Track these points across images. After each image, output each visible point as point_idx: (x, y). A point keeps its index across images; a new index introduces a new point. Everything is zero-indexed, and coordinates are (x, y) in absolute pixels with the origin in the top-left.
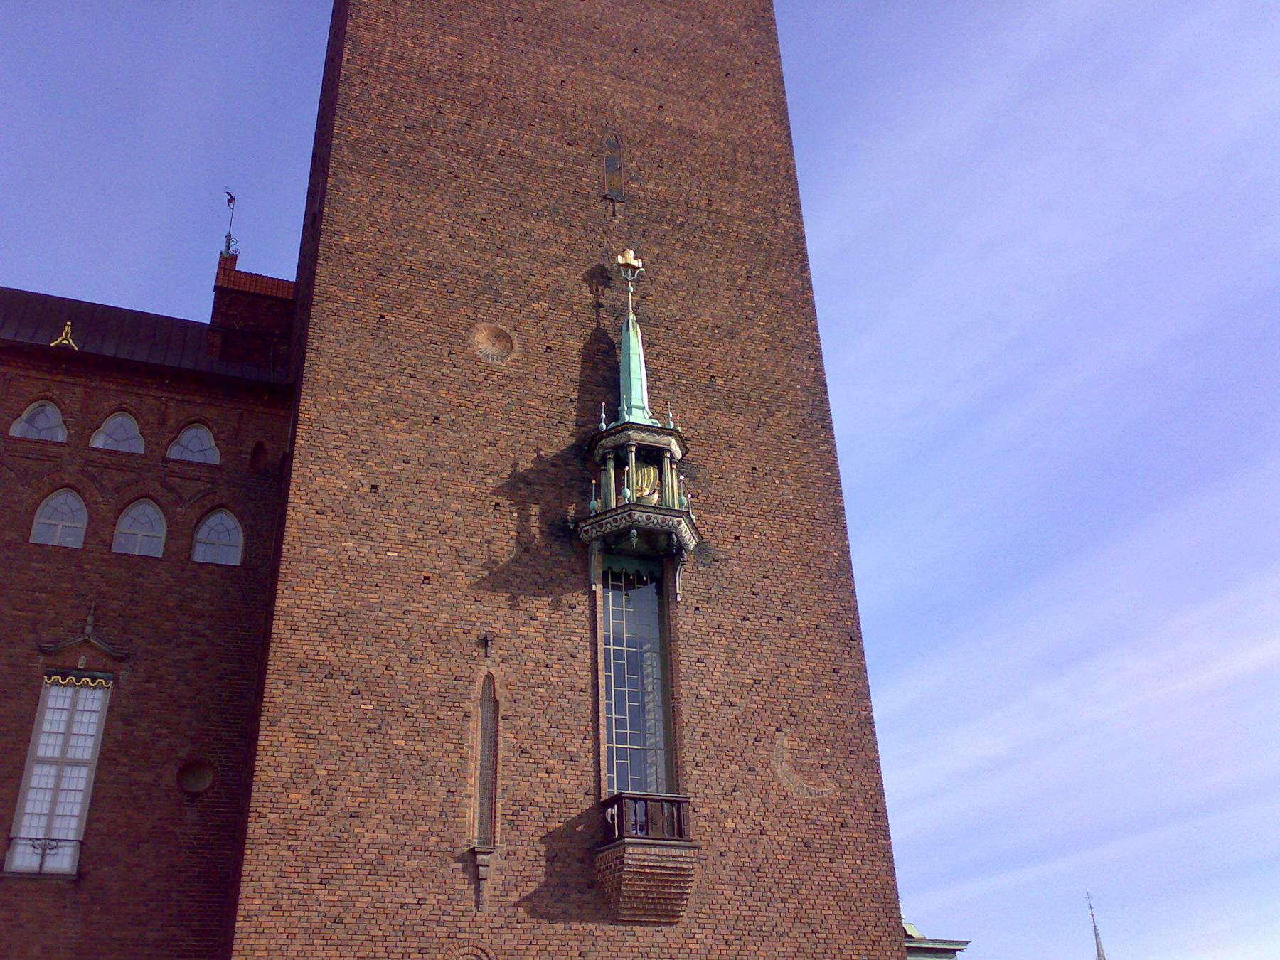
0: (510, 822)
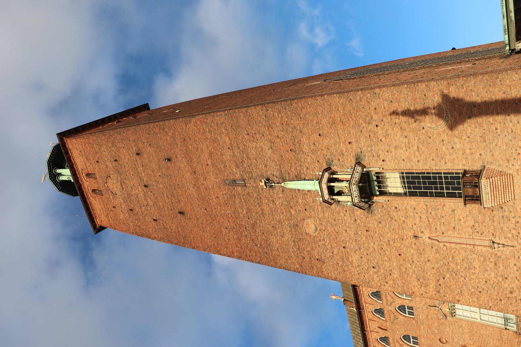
0: (481, 234)
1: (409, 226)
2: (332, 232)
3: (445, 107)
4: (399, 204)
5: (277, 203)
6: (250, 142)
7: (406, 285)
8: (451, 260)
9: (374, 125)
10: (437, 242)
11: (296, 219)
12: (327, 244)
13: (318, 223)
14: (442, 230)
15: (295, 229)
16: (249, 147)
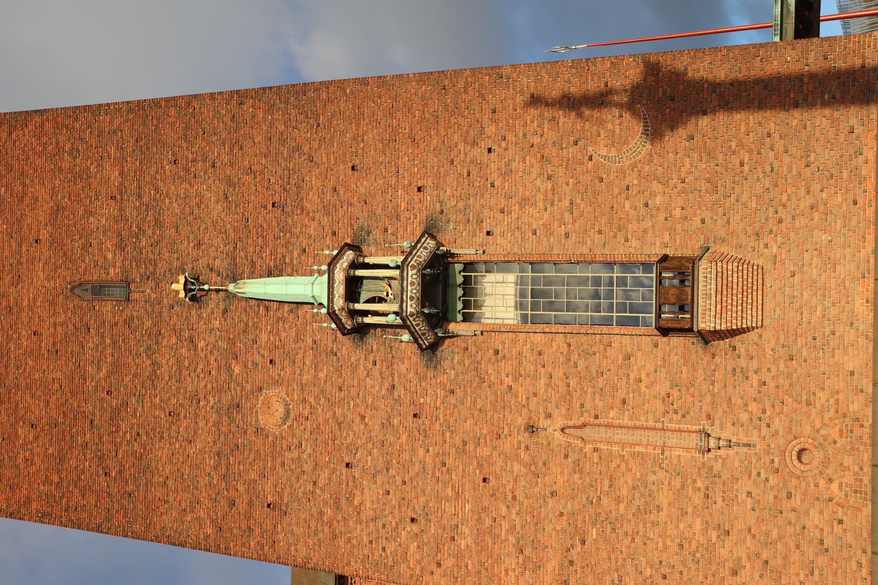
1: (520, 399)
2: (326, 421)
3: (643, 112)
4: (507, 341)
5: (201, 344)
7: (487, 569)
8: (606, 489)
9: (483, 148)
10: (578, 442)
11: (239, 389)
12: (305, 456)
13: (296, 397)
14: (595, 407)
15: (229, 418)
16: (168, 194)
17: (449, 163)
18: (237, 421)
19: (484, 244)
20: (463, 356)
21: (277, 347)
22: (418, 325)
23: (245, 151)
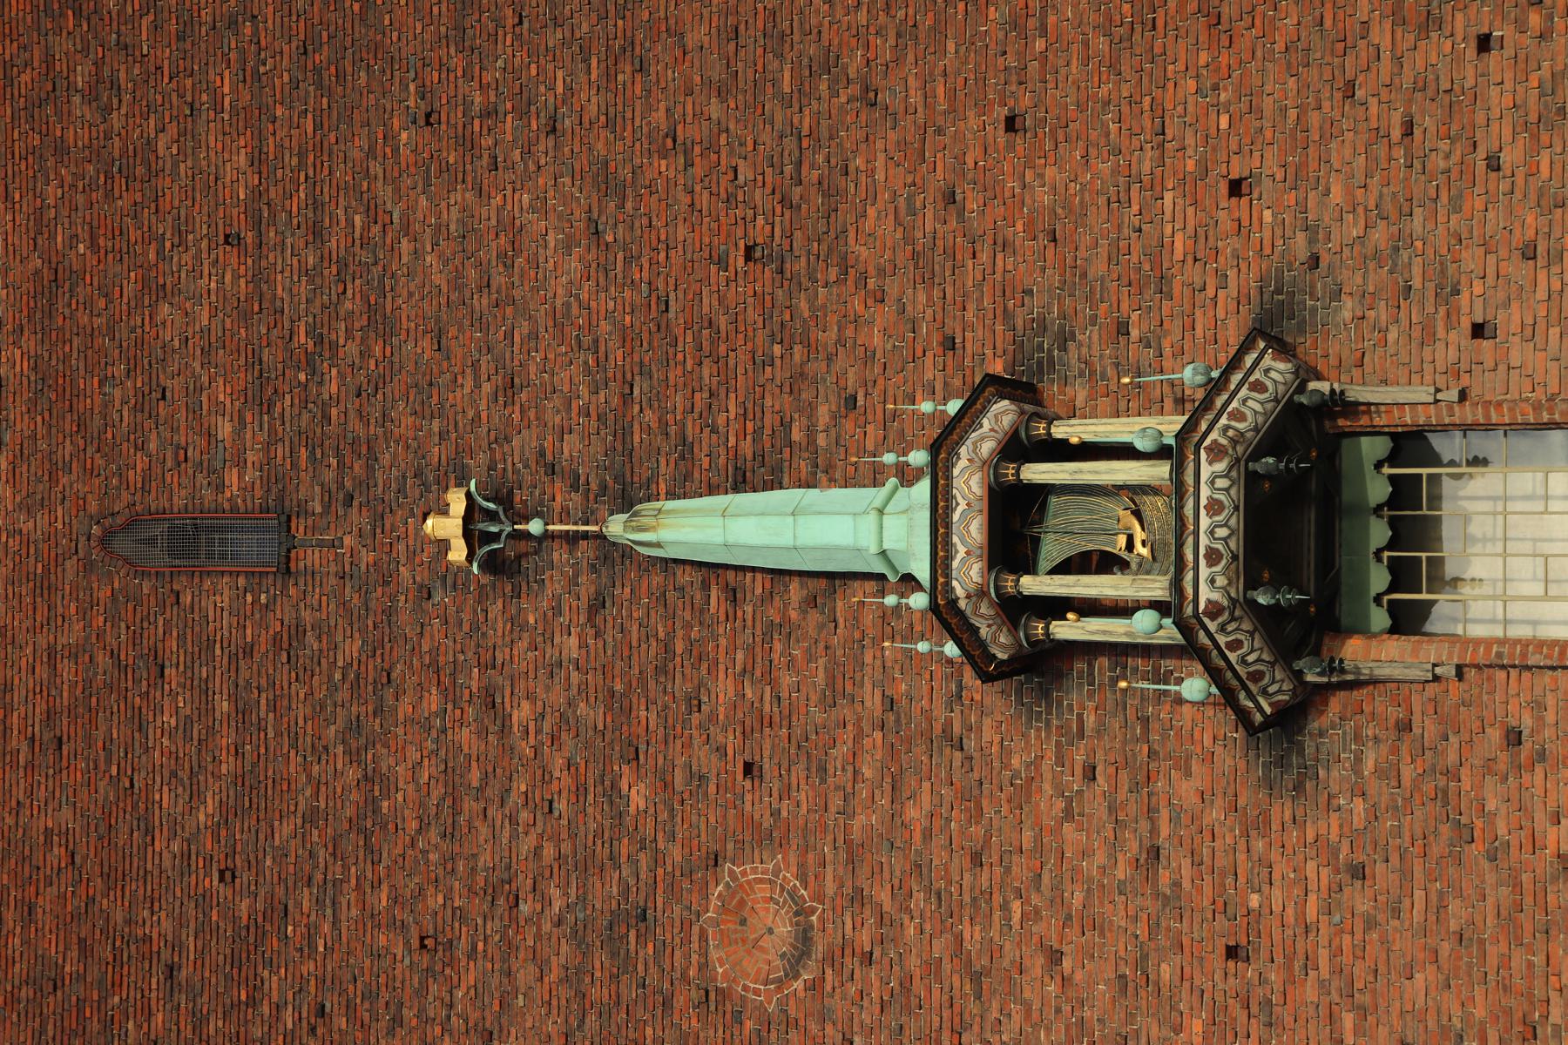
2: (933, 968)
4: (1550, 701)
5: (522, 713)
6: (427, 183)
9: (1459, 38)
11: (644, 860)
13: (830, 888)
15: (614, 955)
16: (406, 228)
17: (1338, 95)
18: (640, 967)
19: (1464, 366)
20: (1395, 750)
21: (766, 721)
22: (1235, 645)
23: (653, 78)
